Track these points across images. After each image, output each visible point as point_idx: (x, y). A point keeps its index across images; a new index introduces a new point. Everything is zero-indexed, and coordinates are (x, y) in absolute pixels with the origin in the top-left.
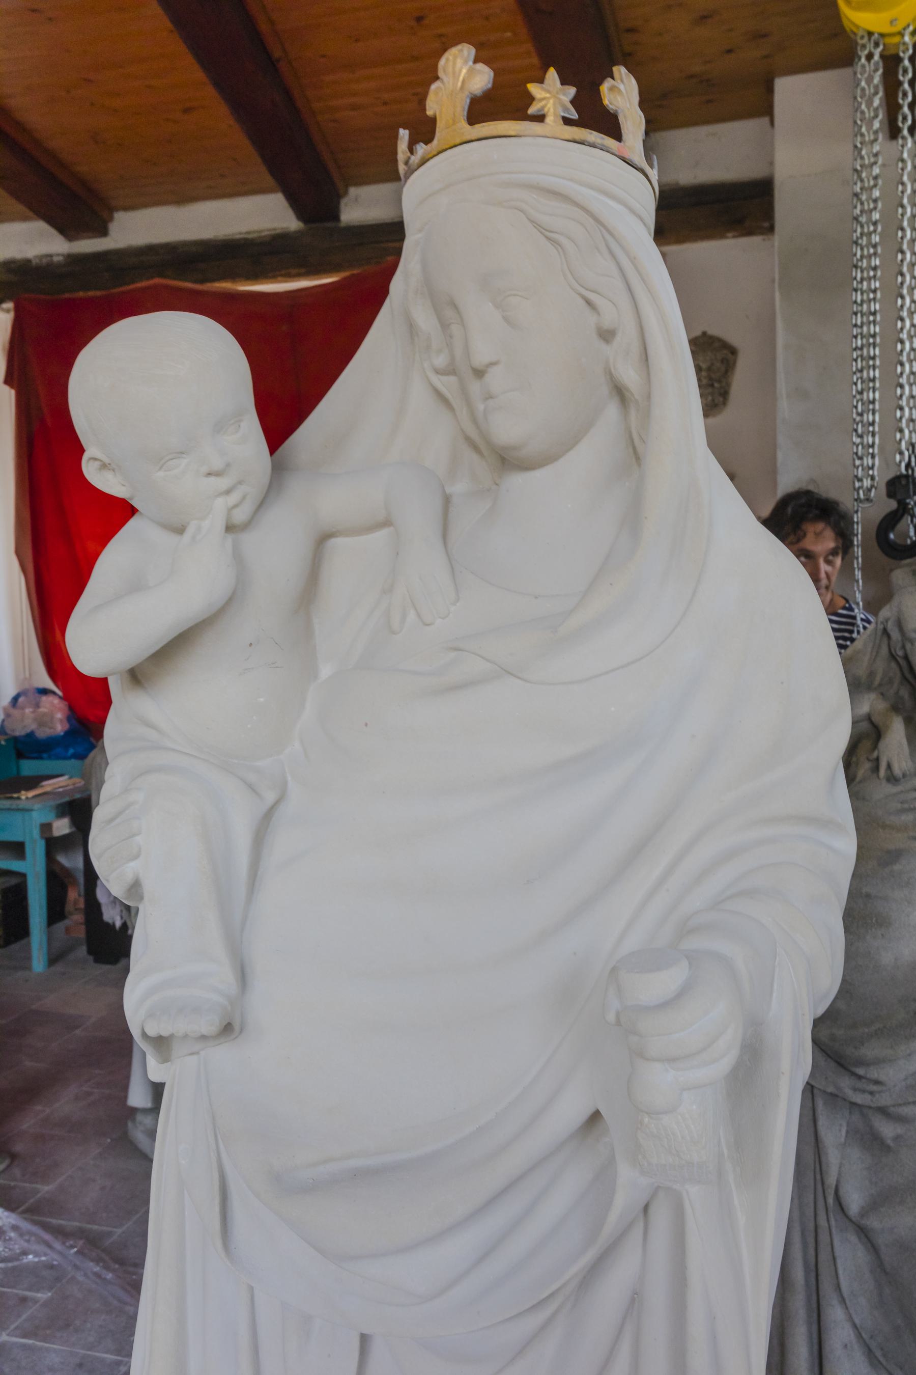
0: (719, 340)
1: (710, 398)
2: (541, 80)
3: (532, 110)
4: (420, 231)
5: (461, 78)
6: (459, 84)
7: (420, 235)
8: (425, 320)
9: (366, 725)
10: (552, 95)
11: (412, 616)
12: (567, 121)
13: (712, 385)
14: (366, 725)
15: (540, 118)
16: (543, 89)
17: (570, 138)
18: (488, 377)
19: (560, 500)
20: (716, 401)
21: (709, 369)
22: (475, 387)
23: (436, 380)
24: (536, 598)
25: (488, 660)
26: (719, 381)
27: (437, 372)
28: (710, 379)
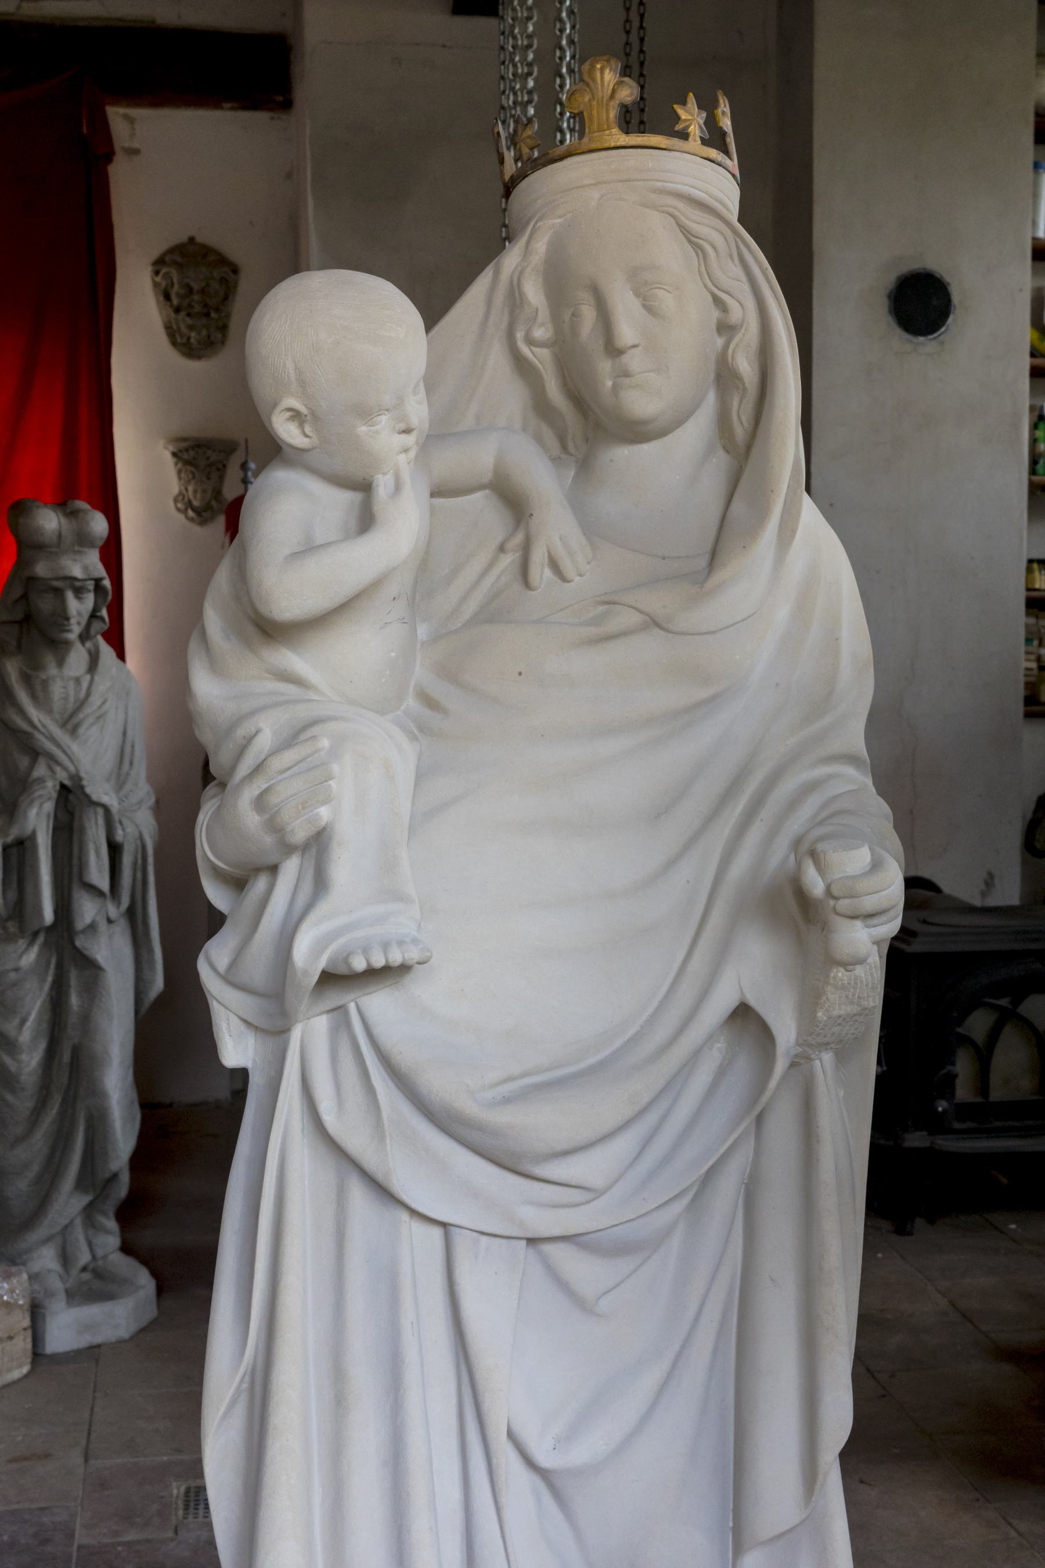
0: (218, 253)
1: (204, 333)
2: (684, 103)
3: (679, 127)
4: (560, 217)
5: (611, 87)
6: (610, 92)
7: (559, 221)
8: (534, 293)
9: (520, 674)
10: (691, 116)
11: (548, 573)
12: (704, 142)
13: (208, 315)
14: (520, 674)
15: (684, 136)
16: (686, 111)
17: (705, 155)
18: (625, 358)
19: (669, 471)
20: (212, 338)
21: (203, 291)
22: (605, 366)
23: (525, 350)
24: (664, 558)
25: (641, 612)
26: (217, 310)
27: (530, 342)
28: (206, 305)
